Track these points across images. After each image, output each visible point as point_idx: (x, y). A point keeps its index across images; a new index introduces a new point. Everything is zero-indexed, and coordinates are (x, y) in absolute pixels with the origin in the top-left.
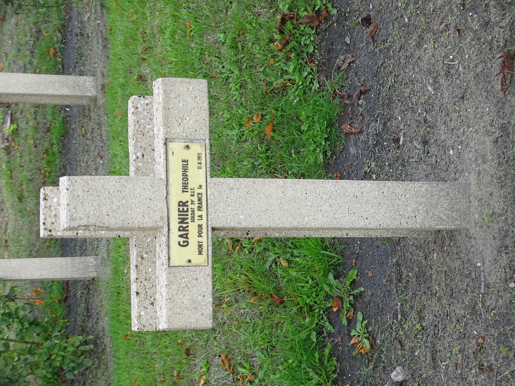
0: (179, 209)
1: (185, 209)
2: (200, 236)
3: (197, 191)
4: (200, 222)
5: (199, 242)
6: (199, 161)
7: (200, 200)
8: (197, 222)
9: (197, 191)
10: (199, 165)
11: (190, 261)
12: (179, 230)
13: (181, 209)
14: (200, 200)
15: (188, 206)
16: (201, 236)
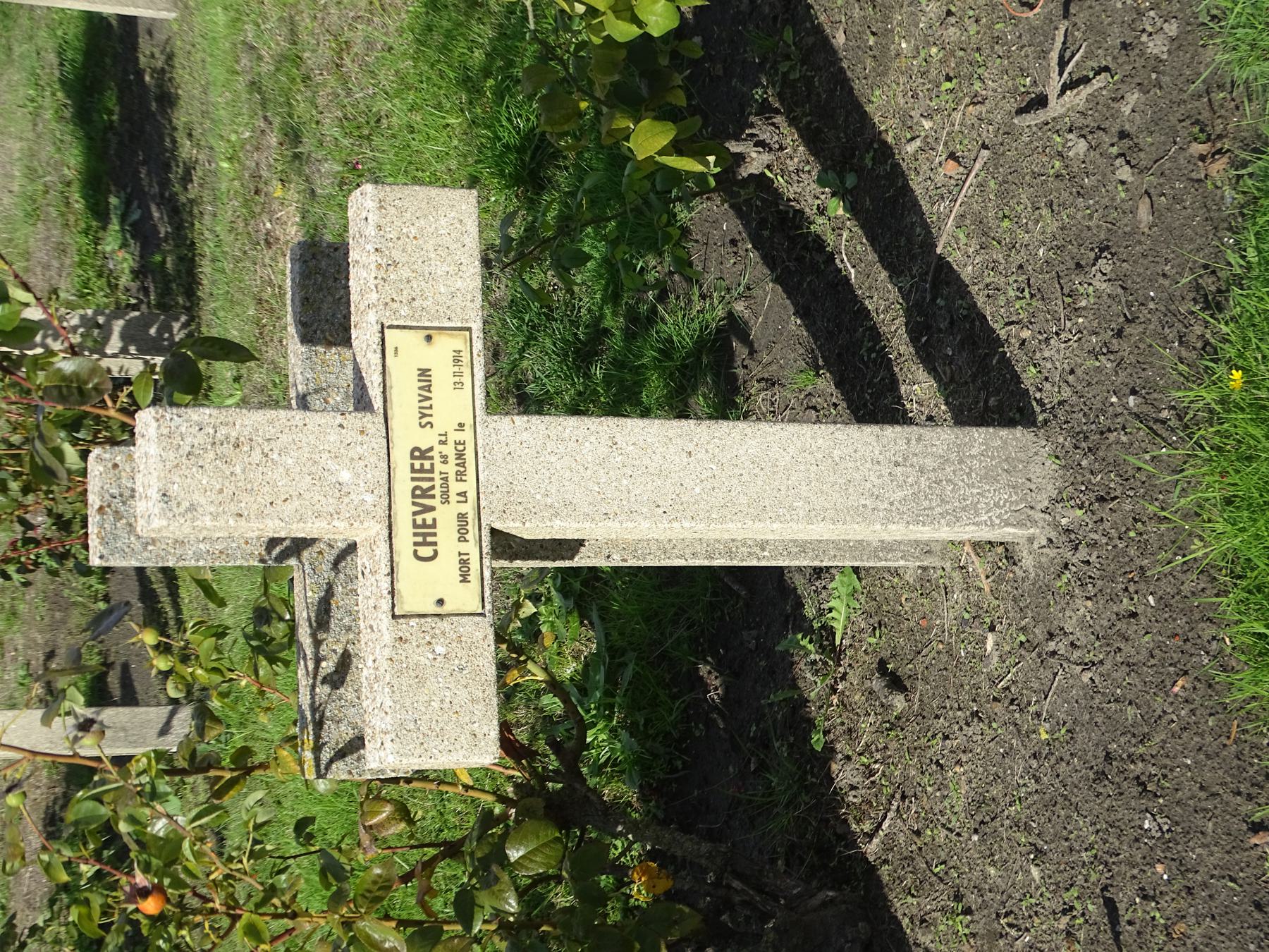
0: (412, 465)
1: (427, 465)
2: (462, 539)
3: (453, 436)
4: (463, 508)
5: (460, 554)
6: (456, 369)
7: (460, 455)
8: (454, 508)
9: (453, 436)
10: (457, 379)
11: (441, 602)
12: (414, 496)
13: (417, 465)
14: (460, 455)
15: (432, 458)
16: (466, 541)
